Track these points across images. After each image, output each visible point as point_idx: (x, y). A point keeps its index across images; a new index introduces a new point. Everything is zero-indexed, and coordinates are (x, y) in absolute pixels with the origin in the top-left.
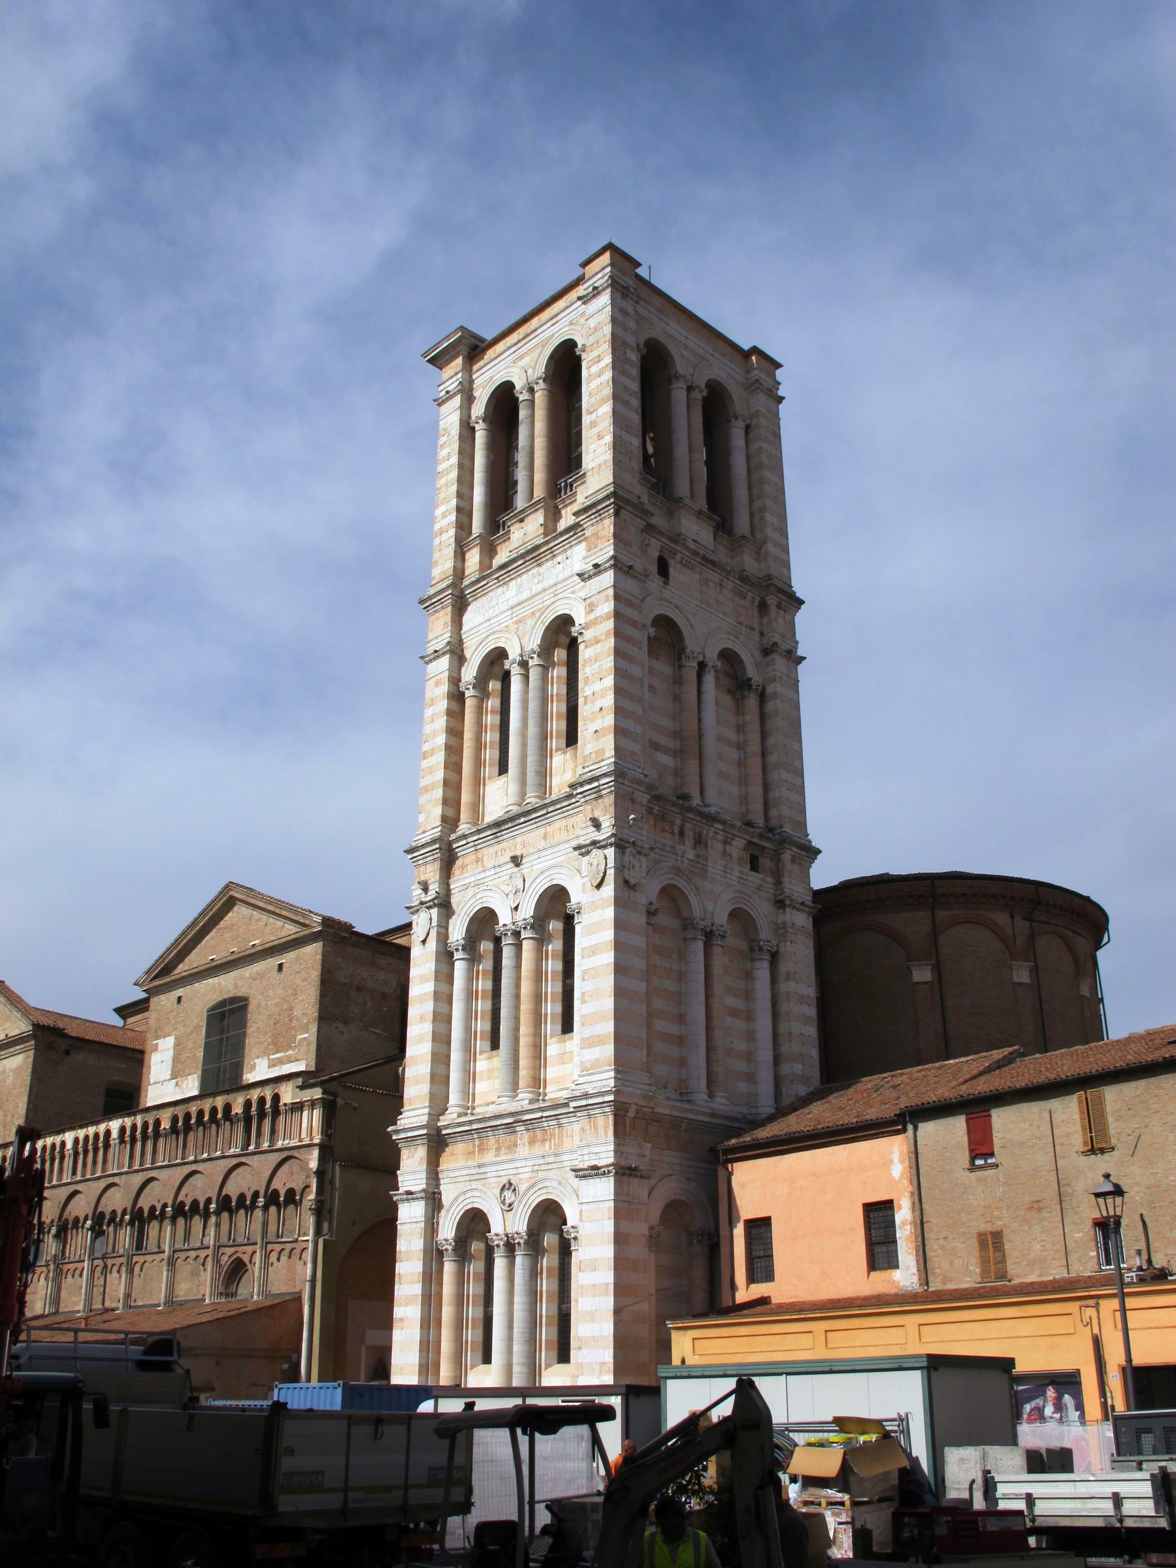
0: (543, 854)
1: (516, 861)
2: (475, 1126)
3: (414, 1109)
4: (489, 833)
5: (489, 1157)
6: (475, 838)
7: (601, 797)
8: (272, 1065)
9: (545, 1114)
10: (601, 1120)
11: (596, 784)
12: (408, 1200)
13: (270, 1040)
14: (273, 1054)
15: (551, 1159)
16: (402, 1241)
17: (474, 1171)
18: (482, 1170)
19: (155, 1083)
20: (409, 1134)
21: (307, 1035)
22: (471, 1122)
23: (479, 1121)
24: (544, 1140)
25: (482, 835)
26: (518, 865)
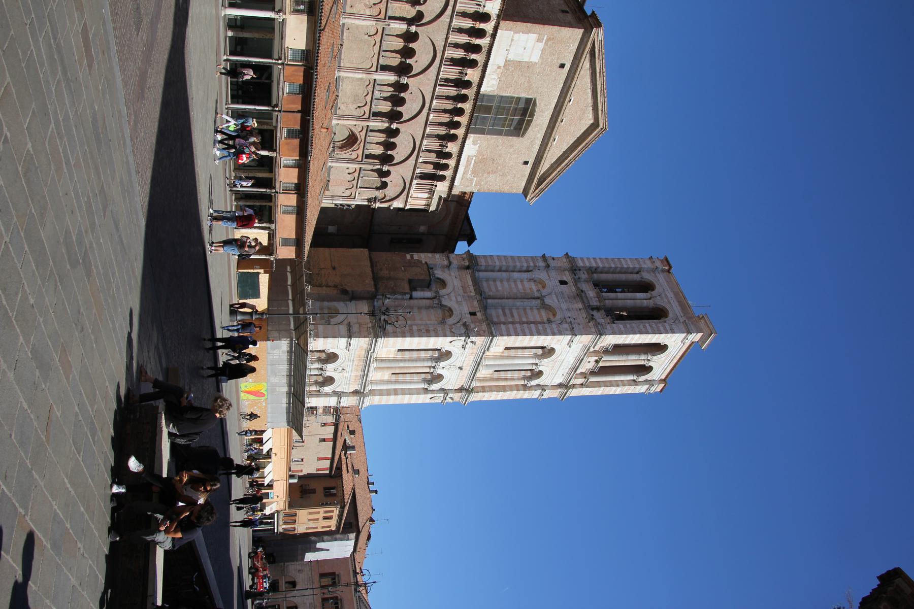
0: (457, 376)
1: (461, 368)
2: (368, 361)
3: (383, 343)
4: (479, 360)
5: (355, 363)
6: (480, 356)
7: (461, 398)
8: (469, 159)
9: (363, 383)
10: (355, 402)
11: (465, 399)
12: (347, 343)
13: (485, 157)
14: (475, 160)
15: (348, 382)
16: (332, 341)
17: (352, 358)
18: (352, 361)
19: (512, 40)
20: (373, 345)
21: (473, 185)
22: (370, 361)
23: (369, 364)
24: (355, 380)
25: (479, 358)
26: (459, 368)
